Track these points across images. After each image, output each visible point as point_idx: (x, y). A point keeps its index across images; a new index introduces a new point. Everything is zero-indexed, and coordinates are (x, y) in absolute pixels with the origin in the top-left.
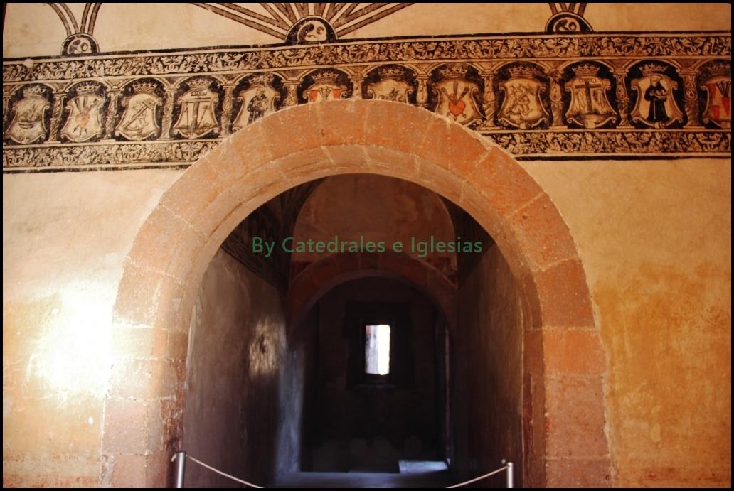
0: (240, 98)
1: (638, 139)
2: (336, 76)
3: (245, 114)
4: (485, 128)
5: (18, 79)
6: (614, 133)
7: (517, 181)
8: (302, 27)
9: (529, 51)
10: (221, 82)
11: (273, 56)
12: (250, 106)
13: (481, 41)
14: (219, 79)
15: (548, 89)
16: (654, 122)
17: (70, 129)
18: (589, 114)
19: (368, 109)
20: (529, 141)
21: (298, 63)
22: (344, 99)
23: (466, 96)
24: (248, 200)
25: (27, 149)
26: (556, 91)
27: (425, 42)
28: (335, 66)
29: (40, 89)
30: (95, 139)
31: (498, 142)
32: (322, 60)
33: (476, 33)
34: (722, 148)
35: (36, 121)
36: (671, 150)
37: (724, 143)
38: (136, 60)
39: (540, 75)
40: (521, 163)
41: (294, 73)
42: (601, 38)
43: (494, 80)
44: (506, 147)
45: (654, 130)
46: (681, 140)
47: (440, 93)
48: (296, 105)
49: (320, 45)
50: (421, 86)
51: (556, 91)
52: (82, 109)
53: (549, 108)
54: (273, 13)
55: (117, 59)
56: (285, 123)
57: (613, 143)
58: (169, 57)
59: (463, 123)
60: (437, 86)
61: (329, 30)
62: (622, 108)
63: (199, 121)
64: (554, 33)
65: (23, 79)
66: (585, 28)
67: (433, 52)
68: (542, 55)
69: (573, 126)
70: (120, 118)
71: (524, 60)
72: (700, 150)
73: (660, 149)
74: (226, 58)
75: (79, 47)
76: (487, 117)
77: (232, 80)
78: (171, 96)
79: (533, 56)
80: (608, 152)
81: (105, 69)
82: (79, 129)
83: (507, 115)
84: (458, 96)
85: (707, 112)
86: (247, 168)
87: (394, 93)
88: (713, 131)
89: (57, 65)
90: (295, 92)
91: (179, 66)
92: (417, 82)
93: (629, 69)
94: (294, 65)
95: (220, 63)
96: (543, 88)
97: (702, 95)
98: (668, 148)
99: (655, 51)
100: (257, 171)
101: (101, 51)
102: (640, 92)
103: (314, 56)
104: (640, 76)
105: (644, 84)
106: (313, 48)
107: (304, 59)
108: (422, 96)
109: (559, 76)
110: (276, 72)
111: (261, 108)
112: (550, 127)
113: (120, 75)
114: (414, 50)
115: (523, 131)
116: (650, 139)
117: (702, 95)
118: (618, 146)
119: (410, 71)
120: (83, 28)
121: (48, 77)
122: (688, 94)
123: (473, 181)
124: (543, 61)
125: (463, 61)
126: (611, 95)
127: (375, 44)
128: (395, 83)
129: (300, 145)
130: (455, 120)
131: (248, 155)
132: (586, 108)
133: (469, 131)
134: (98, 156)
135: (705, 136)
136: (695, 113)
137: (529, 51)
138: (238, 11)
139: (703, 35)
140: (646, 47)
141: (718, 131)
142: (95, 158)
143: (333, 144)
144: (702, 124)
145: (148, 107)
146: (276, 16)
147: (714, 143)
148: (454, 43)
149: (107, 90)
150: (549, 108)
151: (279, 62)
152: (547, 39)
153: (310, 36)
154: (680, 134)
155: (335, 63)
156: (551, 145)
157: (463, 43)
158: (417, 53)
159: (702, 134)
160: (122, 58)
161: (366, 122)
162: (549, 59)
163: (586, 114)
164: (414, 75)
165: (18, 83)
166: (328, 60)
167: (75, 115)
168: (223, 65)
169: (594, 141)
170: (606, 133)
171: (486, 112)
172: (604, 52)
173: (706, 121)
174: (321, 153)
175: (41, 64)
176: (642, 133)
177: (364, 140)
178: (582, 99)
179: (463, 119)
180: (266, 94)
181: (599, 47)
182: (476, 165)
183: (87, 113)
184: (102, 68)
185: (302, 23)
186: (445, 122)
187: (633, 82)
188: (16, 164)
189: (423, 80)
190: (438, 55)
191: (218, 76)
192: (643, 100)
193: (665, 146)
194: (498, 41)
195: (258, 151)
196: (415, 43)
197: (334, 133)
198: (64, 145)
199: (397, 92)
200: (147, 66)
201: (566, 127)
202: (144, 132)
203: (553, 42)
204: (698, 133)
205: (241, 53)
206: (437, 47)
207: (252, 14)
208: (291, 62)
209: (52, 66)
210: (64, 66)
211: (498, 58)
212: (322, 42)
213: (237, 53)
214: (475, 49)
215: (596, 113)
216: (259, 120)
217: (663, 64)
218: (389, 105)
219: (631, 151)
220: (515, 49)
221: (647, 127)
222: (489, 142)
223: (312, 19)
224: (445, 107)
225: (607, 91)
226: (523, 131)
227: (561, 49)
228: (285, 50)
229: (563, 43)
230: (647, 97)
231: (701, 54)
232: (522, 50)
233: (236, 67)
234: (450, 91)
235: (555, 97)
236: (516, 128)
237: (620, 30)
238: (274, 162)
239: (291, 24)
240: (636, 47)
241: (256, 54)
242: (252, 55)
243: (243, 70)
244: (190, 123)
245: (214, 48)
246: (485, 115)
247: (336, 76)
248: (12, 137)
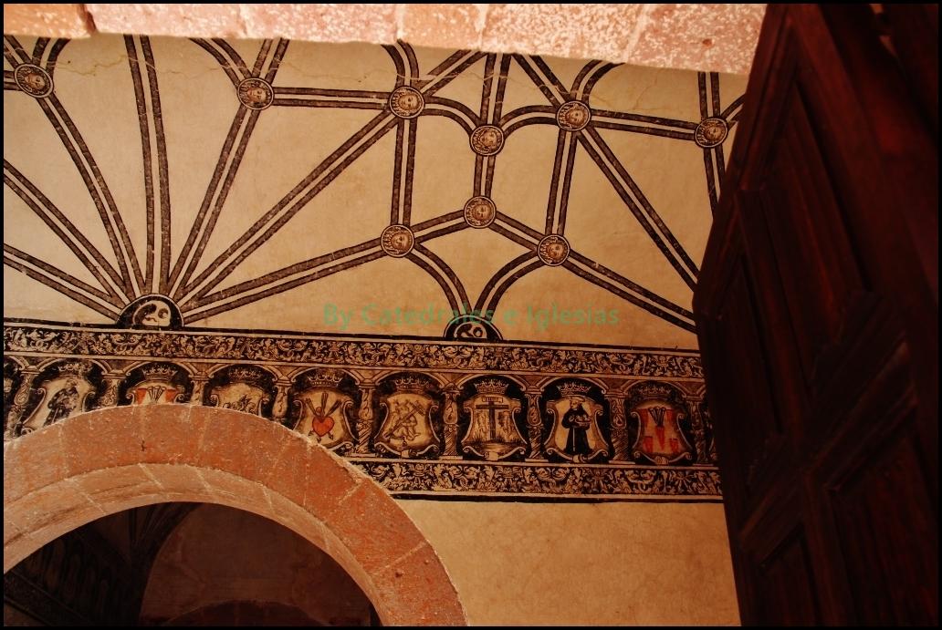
0: (42, 390)
1: (552, 476)
2: (174, 373)
3: (45, 412)
4: (355, 455)
6: (522, 467)
7: (391, 525)
8: (141, 307)
9: (422, 359)
10: (20, 366)
11: (98, 339)
12: (53, 401)
13: (364, 343)
14: (19, 361)
15: (442, 408)
16: (573, 454)
18: (491, 441)
19: (208, 419)
20: (411, 473)
21: (128, 352)
22: (179, 404)
23: (337, 412)
24: (34, 530)
26: (451, 411)
27: (293, 340)
28: (175, 361)
31: (371, 473)
32: (159, 351)
34: (656, 488)
36: (594, 490)
37: (658, 482)
40: (398, 502)
41: (120, 364)
42: (512, 349)
43: (374, 394)
44: (381, 480)
45: (573, 465)
46: (606, 478)
47: (304, 405)
48: (115, 407)
49: (160, 331)
50: (280, 395)
51: (451, 411)
53: (440, 432)
54: (107, 286)
56: (96, 429)
57: (520, 480)
59: (329, 447)
60: (301, 396)
61: (175, 314)
62: (533, 436)
64: (455, 340)
66: (493, 335)
67: (301, 353)
68: (437, 365)
69: (470, 456)
71: (415, 370)
72: (630, 491)
73: (579, 489)
74: (34, 335)
76: (361, 440)
77: (35, 365)
79: (426, 366)
80: (513, 492)
83: (386, 439)
84: (326, 411)
85: (638, 445)
86: (31, 485)
87: (244, 401)
88: (645, 467)
90: (116, 390)
93: (545, 388)
94: (121, 354)
95: (24, 341)
96: (436, 406)
97: (632, 423)
98: (590, 488)
99: (577, 368)
100: (44, 490)
102: (557, 416)
103: (150, 345)
104: (558, 397)
105: (563, 407)
106: (151, 334)
107: (137, 348)
108: (280, 407)
109: (458, 392)
110: (96, 360)
111: (67, 406)
112: (441, 457)
114: (278, 348)
115: (404, 460)
116: (567, 475)
117: (632, 423)
118: (527, 485)
119: (269, 375)
122: (615, 420)
123: (333, 523)
124: (439, 373)
125: (338, 366)
126: (521, 420)
127: (230, 337)
128: (249, 389)
129: (111, 459)
130: (319, 441)
131: (36, 467)
132: (489, 434)
133: (335, 456)
135: (635, 473)
136: (623, 444)
137: (422, 359)
138: (62, 278)
139: (632, 351)
140: (567, 362)
141: (651, 467)
143: (155, 463)
144: (631, 458)
146: (110, 290)
147: (647, 482)
148: (329, 343)
150: (440, 432)
151: (104, 348)
152: (445, 346)
153: (149, 319)
154: (605, 471)
155: (175, 357)
156: (440, 480)
157: (341, 344)
158: (281, 352)
159: (632, 471)
161: (202, 435)
162: (446, 371)
163: (488, 442)
164: (273, 380)
166: (167, 351)
168: (28, 344)
169: (496, 476)
170: (512, 467)
171: (360, 434)
172: (514, 366)
173: (637, 454)
174: (141, 473)
176: (557, 468)
177: (197, 460)
178: (484, 423)
179: (329, 441)
180: (78, 388)
181: (509, 359)
182: (340, 502)
185: (142, 302)
187: (549, 403)
189: (284, 387)
190: (308, 358)
191: (18, 357)
192: (560, 427)
193: (586, 485)
194: (385, 345)
195: (50, 463)
196: (280, 340)
197: (159, 446)
201: (461, 458)
203: (453, 350)
204: (627, 469)
205: (56, 331)
206: (307, 346)
207: (79, 284)
208: (119, 350)
211: (382, 365)
212: (163, 328)
213: (50, 331)
215: (501, 441)
216: (61, 421)
217: (586, 383)
218: (236, 416)
219: (542, 491)
220: (405, 356)
221: (564, 461)
222: (359, 471)
223: (155, 298)
224: (308, 424)
226: (404, 460)
227: (462, 360)
228: (114, 333)
229: (466, 352)
230: (566, 424)
231: (632, 374)
232: (413, 357)
233: (45, 348)
234: (317, 404)
235: (450, 418)
236: (396, 457)
237: (535, 340)
238: (72, 480)
239: (127, 302)
240: (554, 362)
241: (75, 334)
242: (70, 335)
243: (53, 353)
245: (21, 321)
246: (358, 437)
247: (174, 373)
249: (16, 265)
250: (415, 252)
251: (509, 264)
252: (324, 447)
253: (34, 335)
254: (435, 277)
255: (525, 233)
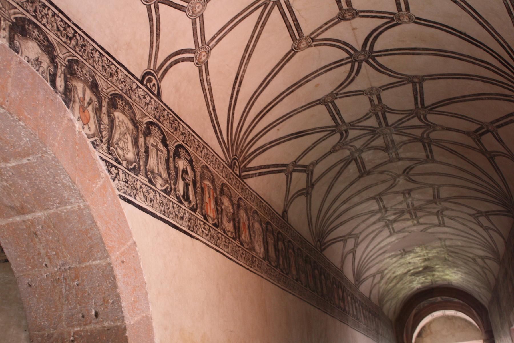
31: (109, 171)
33: (101, 45)
39: (134, 119)
53: (138, 154)
87: (38, 62)
92: (57, 64)
128: (40, 51)
133: (91, 146)
186: (75, 126)
189: (62, 65)
199: (41, 63)
203: (142, 92)
214: (99, 61)
225: (166, 159)
250: (153, 6)
251: (182, 50)
252: (86, 136)
254: (151, 32)
255: (201, 36)
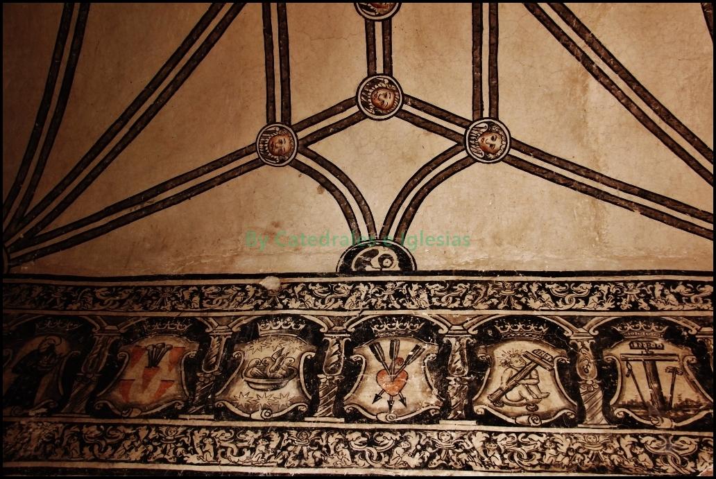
5: (246, 307)
10: (687, 329)
17: (367, 393)
25: (265, 430)
29: (293, 325)
30: (425, 418)
35: (284, 377)
38: (494, 287)
52: (389, 361)
55: (456, 283)
58: (562, 284)
63: (666, 392)
65: (257, 307)
70: (480, 382)
74: (680, 289)
75: (375, 262)
78: (583, 346)
81: (430, 298)
82: (386, 397)
89: (330, 288)
91: (586, 300)
95: (671, 297)
101: (420, 268)
113: (465, 309)
120: (385, 232)
121: (311, 305)
134: (440, 452)
142: (432, 457)
145: (538, 364)
149: (440, 332)
160: (465, 282)
165: (247, 312)
167: (375, 371)
175: (297, 284)
183: (400, 371)
184: (424, 295)
188: (236, 459)
191: (677, 318)
198: (353, 426)
200: (519, 296)
202: (542, 408)
209: (318, 289)
210: (344, 290)
244: (647, 398)
245: (652, 272)
248: (229, 406)
249: (623, 203)
253: (680, 289)
